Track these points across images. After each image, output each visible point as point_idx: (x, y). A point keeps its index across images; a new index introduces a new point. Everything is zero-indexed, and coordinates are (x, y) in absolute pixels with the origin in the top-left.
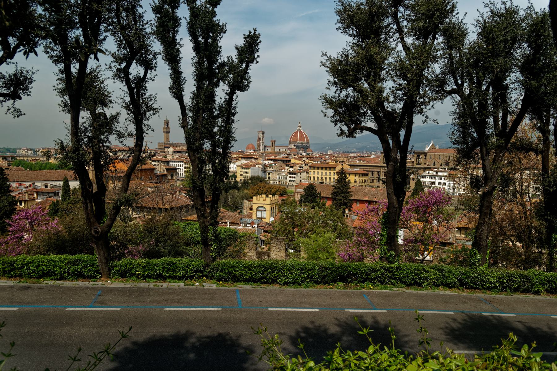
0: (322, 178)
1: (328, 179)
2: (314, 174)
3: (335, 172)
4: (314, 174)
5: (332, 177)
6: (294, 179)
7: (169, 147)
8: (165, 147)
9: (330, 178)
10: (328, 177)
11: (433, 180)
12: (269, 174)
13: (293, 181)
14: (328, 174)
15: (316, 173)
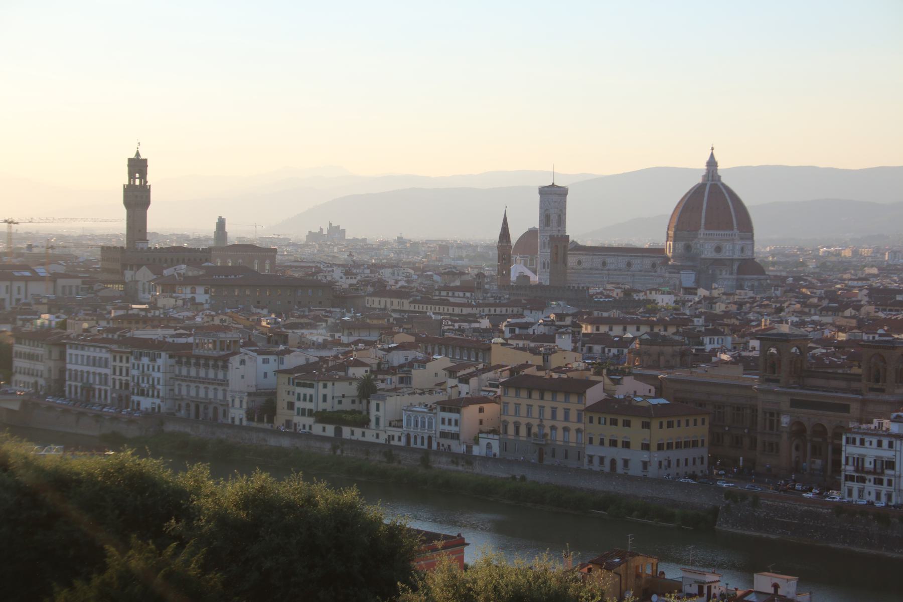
0: (541, 426)
1: (560, 435)
2: (517, 413)
3: (582, 407)
4: (517, 413)
5: (573, 426)
6: (453, 429)
7: (139, 267)
8: (124, 266)
9: (566, 429)
10: (560, 425)
11: (886, 454)
12: (378, 410)
13: (455, 436)
14: (560, 415)
15: (523, 410)
